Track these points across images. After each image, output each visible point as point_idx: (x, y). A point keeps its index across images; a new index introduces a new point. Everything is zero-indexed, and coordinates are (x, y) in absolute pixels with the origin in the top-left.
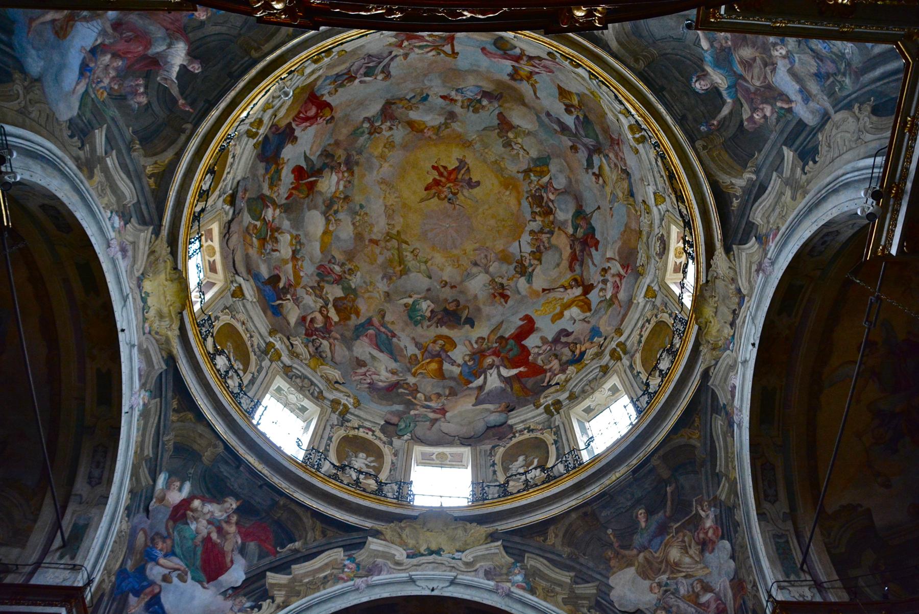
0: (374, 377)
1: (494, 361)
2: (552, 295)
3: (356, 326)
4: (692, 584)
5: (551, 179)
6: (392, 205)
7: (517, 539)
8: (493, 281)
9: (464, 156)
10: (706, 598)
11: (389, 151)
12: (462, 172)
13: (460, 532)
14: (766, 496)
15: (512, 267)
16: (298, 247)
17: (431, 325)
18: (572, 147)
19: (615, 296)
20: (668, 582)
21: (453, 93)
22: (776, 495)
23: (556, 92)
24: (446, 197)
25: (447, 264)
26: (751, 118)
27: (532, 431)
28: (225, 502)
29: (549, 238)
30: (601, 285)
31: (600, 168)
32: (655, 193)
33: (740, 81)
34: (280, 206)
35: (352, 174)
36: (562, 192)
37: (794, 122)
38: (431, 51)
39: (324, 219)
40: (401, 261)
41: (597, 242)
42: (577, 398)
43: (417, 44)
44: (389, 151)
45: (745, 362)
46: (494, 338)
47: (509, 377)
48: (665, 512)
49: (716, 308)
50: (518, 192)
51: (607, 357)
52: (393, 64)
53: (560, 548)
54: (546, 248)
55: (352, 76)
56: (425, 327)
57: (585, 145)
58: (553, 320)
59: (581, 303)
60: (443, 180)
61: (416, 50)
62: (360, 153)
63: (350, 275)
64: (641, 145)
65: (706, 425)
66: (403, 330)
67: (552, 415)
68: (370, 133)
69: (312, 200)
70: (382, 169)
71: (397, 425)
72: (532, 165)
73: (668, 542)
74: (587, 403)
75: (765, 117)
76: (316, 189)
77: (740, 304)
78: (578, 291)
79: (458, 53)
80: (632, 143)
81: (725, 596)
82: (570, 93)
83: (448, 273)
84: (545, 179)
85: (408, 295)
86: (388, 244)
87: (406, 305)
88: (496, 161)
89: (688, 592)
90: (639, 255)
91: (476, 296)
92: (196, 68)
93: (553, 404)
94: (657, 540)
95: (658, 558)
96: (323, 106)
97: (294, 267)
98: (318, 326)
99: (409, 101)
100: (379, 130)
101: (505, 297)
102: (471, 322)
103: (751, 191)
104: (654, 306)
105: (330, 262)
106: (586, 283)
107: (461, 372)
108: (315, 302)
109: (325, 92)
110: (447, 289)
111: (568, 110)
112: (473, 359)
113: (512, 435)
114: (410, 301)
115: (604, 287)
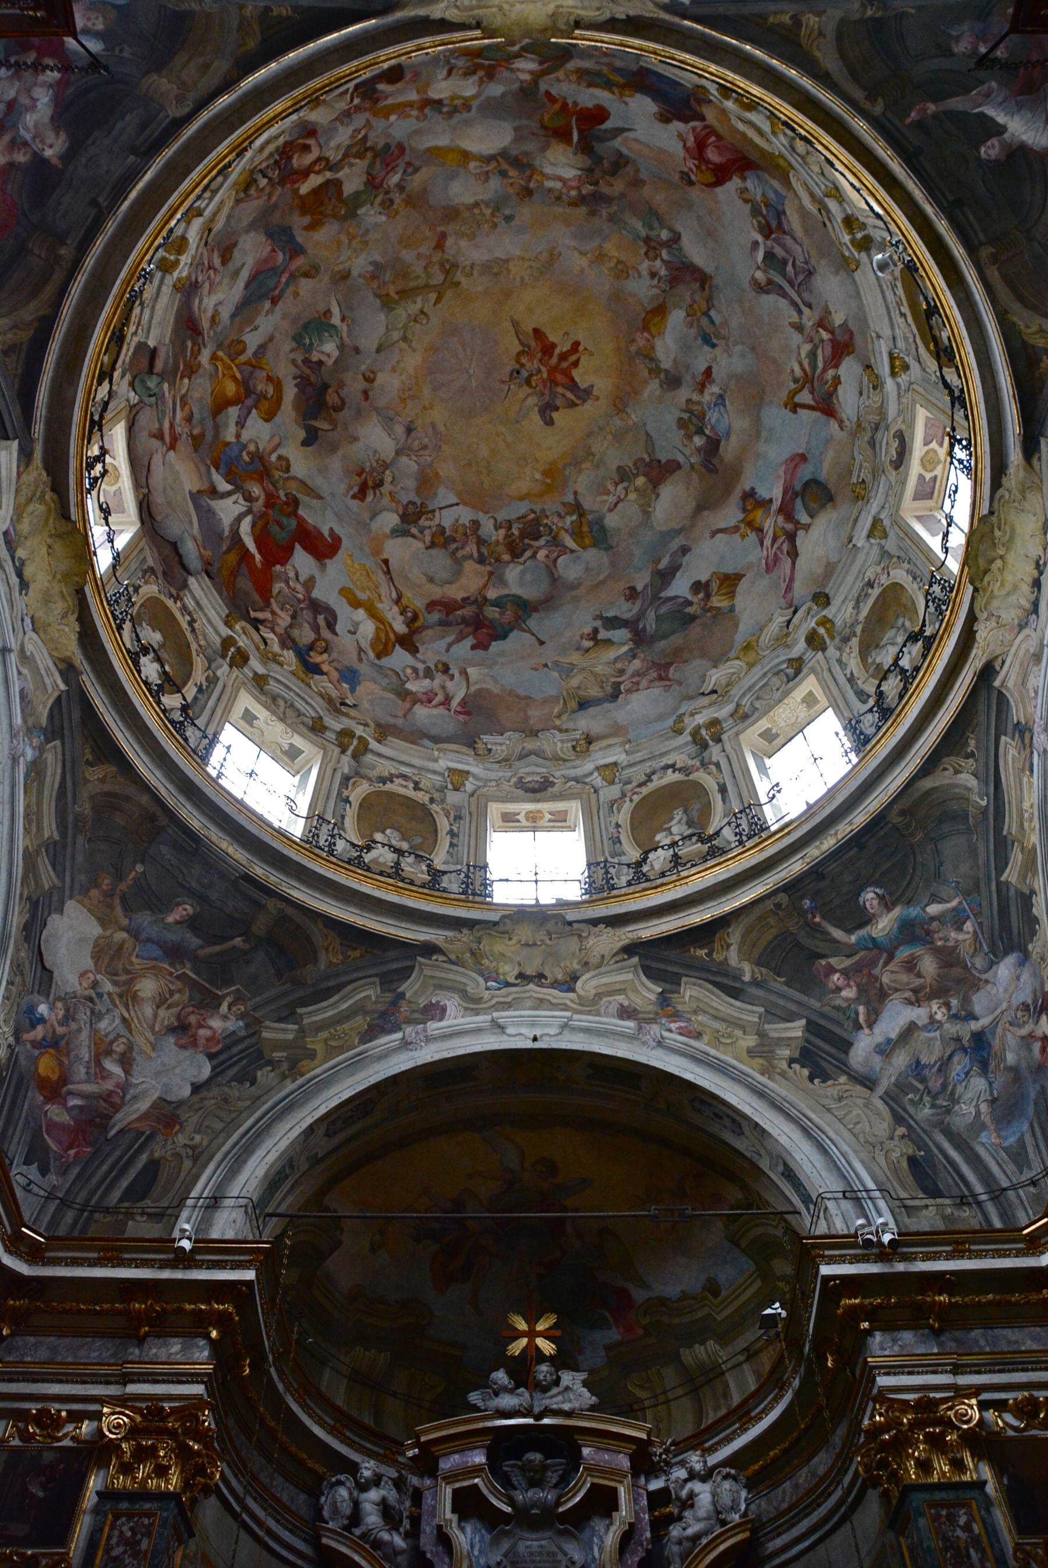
0: (207, 285)
1: (257, 500)
2: (381, 578)
3: (290, 228)
4: (119, 1036)
5: (572, 551)
6: (509, 271)
7: (76, 715)
8: (385, 466)
9: (597, 399)
10: (113, 1067)
11: (610, 269)
12: (569, 395)
13: (59, 606)
14: (333, 1123)
15: (412, 496)
16: (445, 109)
17: (296, 366)
18: (633, 589)
19: (415, 699)
20: (106, 996)
21: (715, 389)
22: (335, 1133)
23: (729, 568)
24: (523, 365)
25: (403, 377)
26: (832, 970)
27: (193, 630)
28: (57, 130)
29: (471, 557)
30: (421, 667)
31: (609, 642)
32: (615, 764)
33: (885, 955)
34: (535, 82)
35: (574, 204)
36: (552, 574)
37: (844, 1035)
38: (803, 369)
39: (492, 152)
40: (405, 294)
41: (486, 648)
42: (262, 690)
43: (819, 352)
44: (610, 269)
45: (499, 1027)
46: (293, 487)
47: (240, 539)
48: (202, 947)
49: (535, 944)
50: (541, 495)
51: (338, 727)
52: (783, 303)
53: (86, 795)
54: (454, 553)
55: (771, 232)
56: (292, 356)
57: (641, 615)
58: (345, 592)
59: (383, 636)
60: (554, 361)
61: (807, 347)
62: (612, 219)
63: (382, 203)
64: (689, 738)
65: (357, 969)
66: (284, 317)
67: (224, 657)
68: (647, 240)
69: (533, 134)
70: (576, 254)
71: (151, 370)
72: (590, 517)
73: (161, 969)
74: (261, 713)
75: (839, 989)
76: (553, 141)
77: (556, 984)
78: (400, 626)
79: (795, 412)
80: (690, 724)
81: (135, 1098)
82: (731, 594)
83: (389, 383)
84: (569, 542)
85: (348, 314)
86: (437, 267)
87: (328, 313)
88: (593, 455)
89: (107, 1035)
90: (499, 739)
91: (355, 439)
92: (990, 150)
93: (239, 650)
94: (157, 952)
95: (131, 963)
96: (720, 175)
97: (410, 104)
98: (294, 161)
99: (706, 314)
100: (651, 254)
101: (361, 494)
102: (311, 439)
103: (726, 975)
104: (442, 789)
105: (409, 164)
106: (416, 638)
107: (229, 444)
108: (338, 147)
109: (749, 184)
110: (362, 385)
111: (697, 587)
112: (252, 459)
113: (174, 592)
114: (336, 320)
115: (421, 674)
